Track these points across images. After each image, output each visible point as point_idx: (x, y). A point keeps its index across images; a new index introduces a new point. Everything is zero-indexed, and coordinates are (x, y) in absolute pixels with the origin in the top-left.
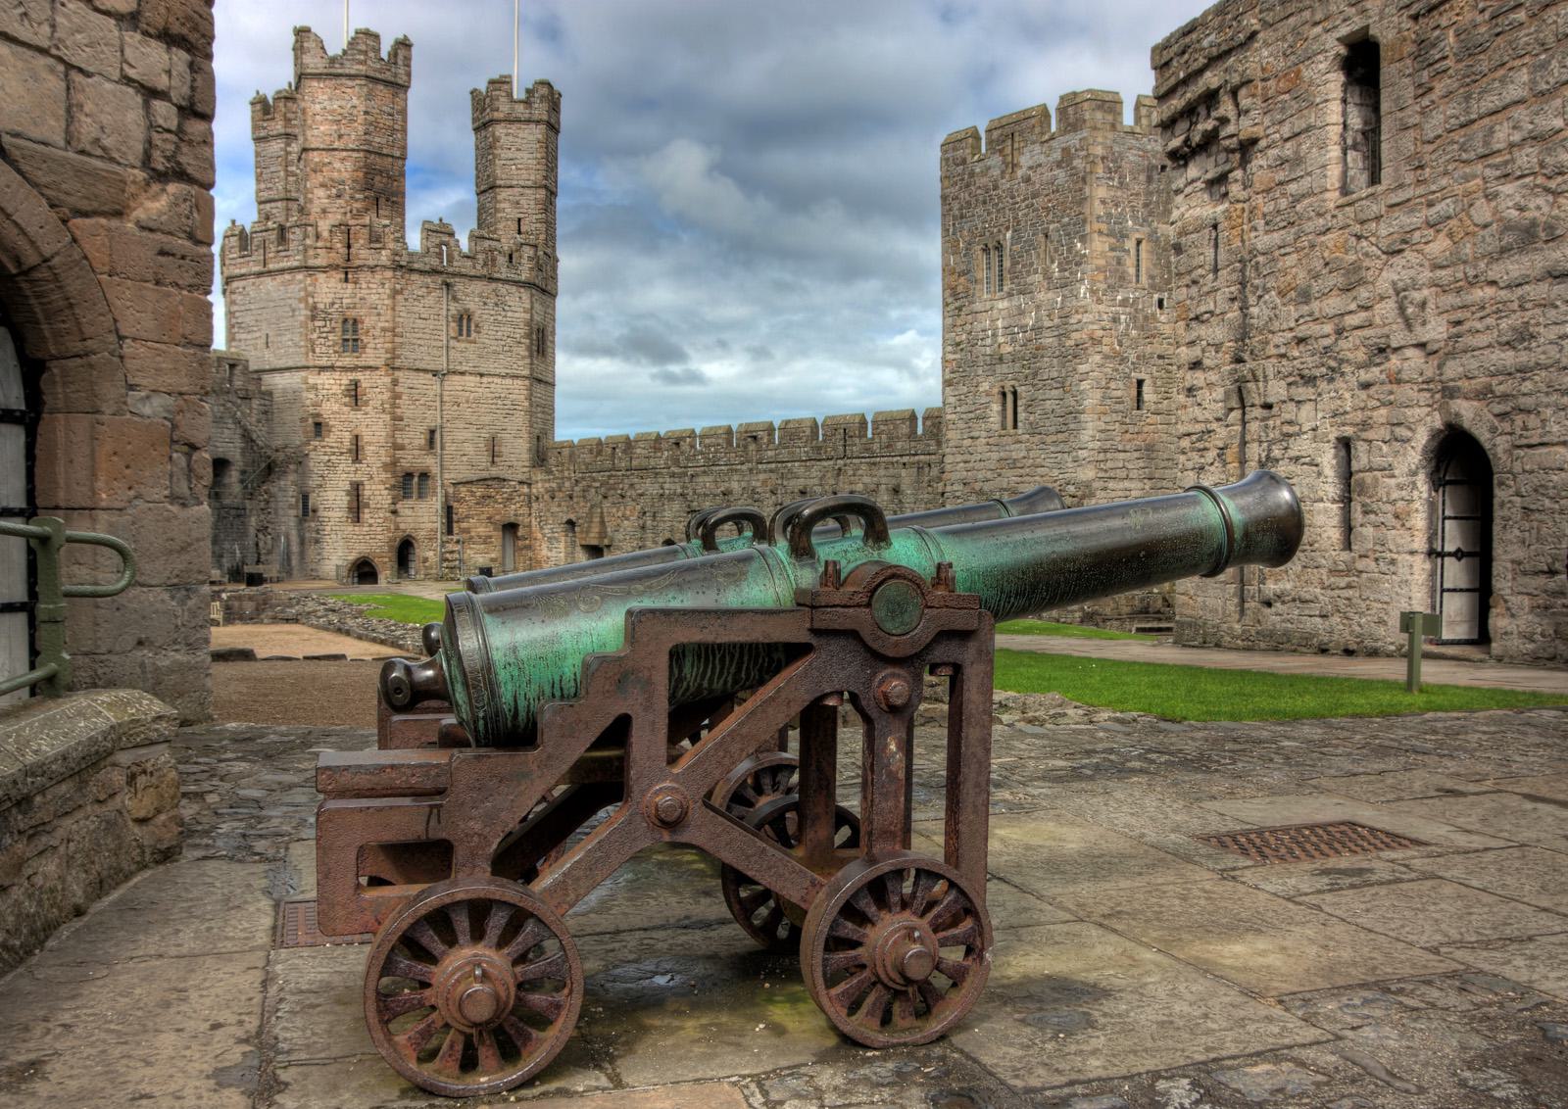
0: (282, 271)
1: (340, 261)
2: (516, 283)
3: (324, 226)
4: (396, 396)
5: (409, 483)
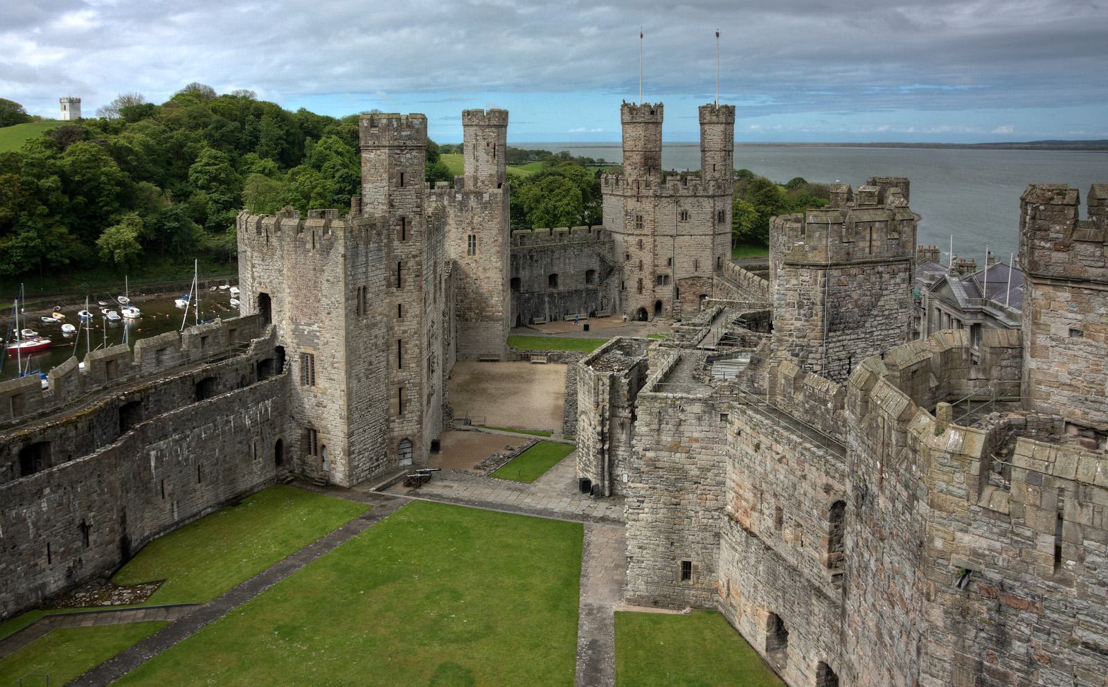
0: (617, 195)
1: (635, 194)
2: (708, 197)
3: (630, 180)
4: (655, 246)
5: (661, 280)
